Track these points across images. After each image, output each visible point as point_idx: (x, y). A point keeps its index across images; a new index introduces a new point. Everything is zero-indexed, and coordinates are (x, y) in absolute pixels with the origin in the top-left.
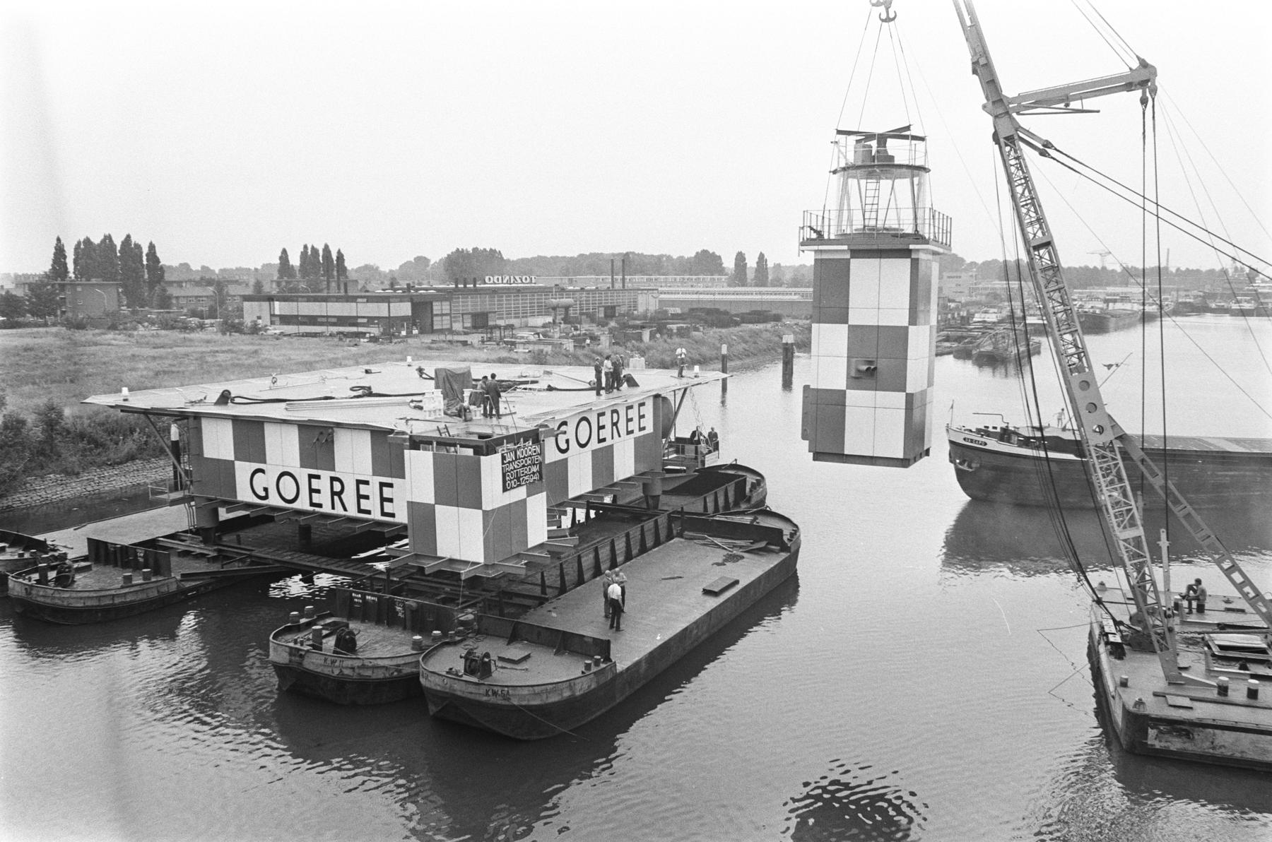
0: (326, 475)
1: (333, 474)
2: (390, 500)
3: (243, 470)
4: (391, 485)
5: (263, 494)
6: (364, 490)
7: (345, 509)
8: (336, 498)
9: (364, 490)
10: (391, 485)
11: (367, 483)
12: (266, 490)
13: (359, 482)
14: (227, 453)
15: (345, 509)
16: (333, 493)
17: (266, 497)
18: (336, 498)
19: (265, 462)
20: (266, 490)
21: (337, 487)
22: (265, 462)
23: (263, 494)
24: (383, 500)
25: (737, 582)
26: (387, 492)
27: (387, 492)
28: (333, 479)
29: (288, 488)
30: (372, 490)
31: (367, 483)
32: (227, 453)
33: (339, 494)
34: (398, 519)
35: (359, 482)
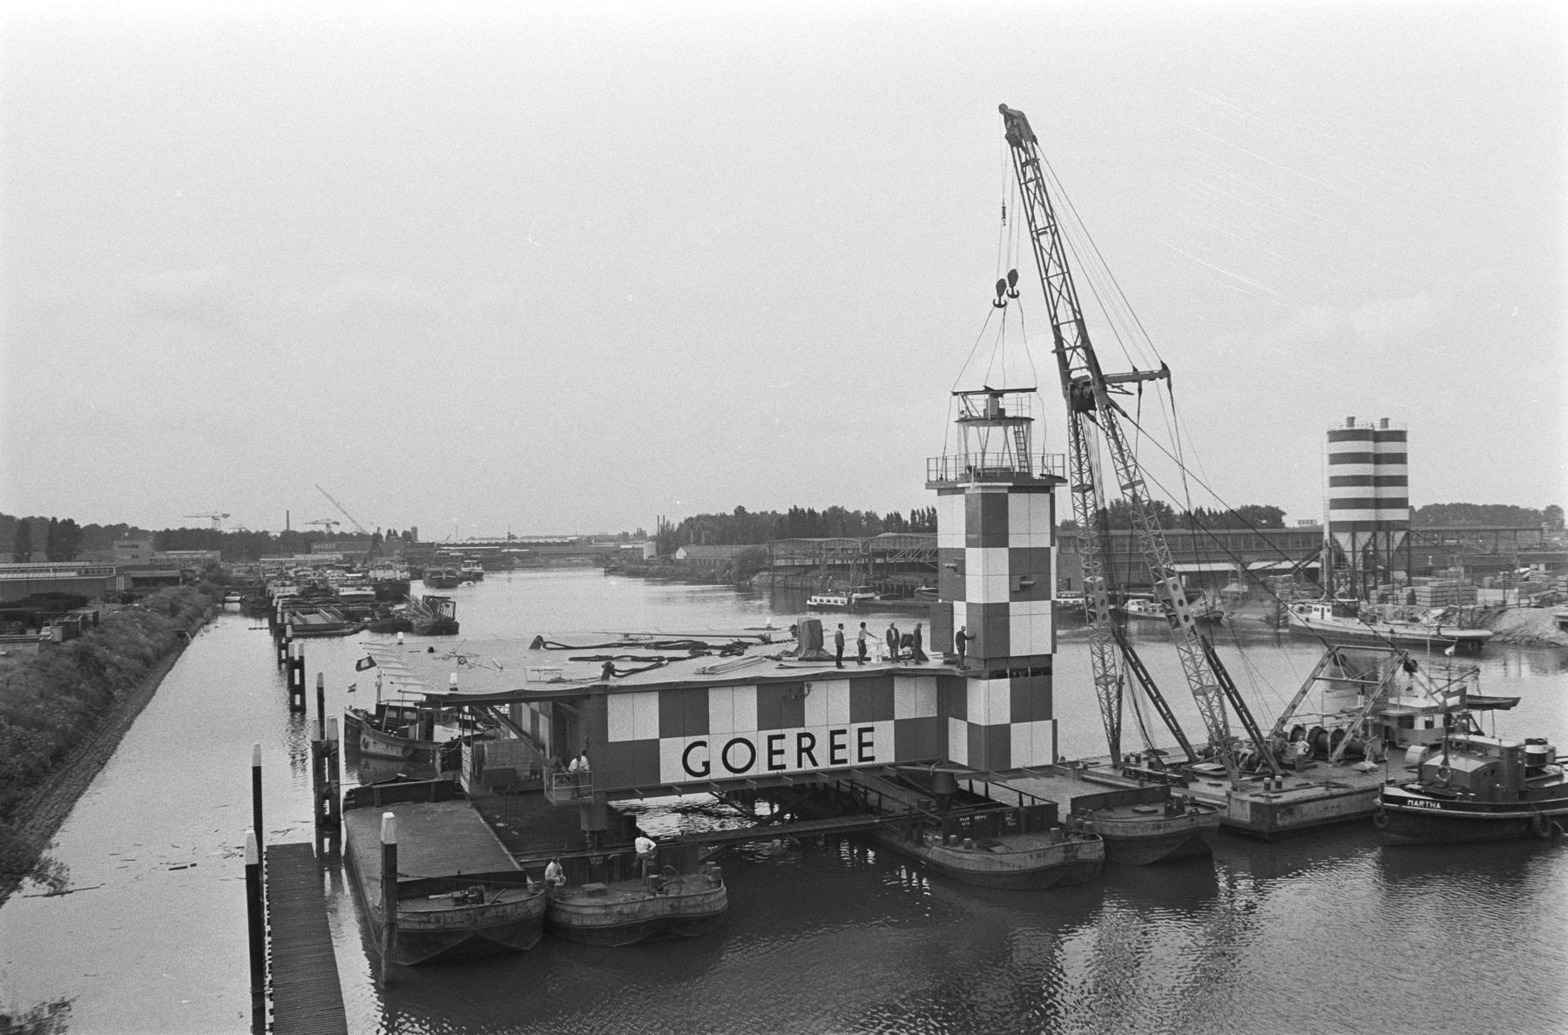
0: (791, 734)
1: (801, 730)
3: (671, 749)
6: (839, 740)
8: (804, 755)
9: (839, 740)
12: (706, 764)
13: (833, 733)
16: (800, 750)
17: (707, 772)
18: (804, 755)
19: (707, 732)
20: (706, 764)
21: (806, 742)
22: (707, 732)
26: (866, 737)
27: (866, 737)
28: (800, 736)
29: (739, 756)
30: (850, 740)
33: (808, 750)
34: (876, 762)
35: (833, 733)
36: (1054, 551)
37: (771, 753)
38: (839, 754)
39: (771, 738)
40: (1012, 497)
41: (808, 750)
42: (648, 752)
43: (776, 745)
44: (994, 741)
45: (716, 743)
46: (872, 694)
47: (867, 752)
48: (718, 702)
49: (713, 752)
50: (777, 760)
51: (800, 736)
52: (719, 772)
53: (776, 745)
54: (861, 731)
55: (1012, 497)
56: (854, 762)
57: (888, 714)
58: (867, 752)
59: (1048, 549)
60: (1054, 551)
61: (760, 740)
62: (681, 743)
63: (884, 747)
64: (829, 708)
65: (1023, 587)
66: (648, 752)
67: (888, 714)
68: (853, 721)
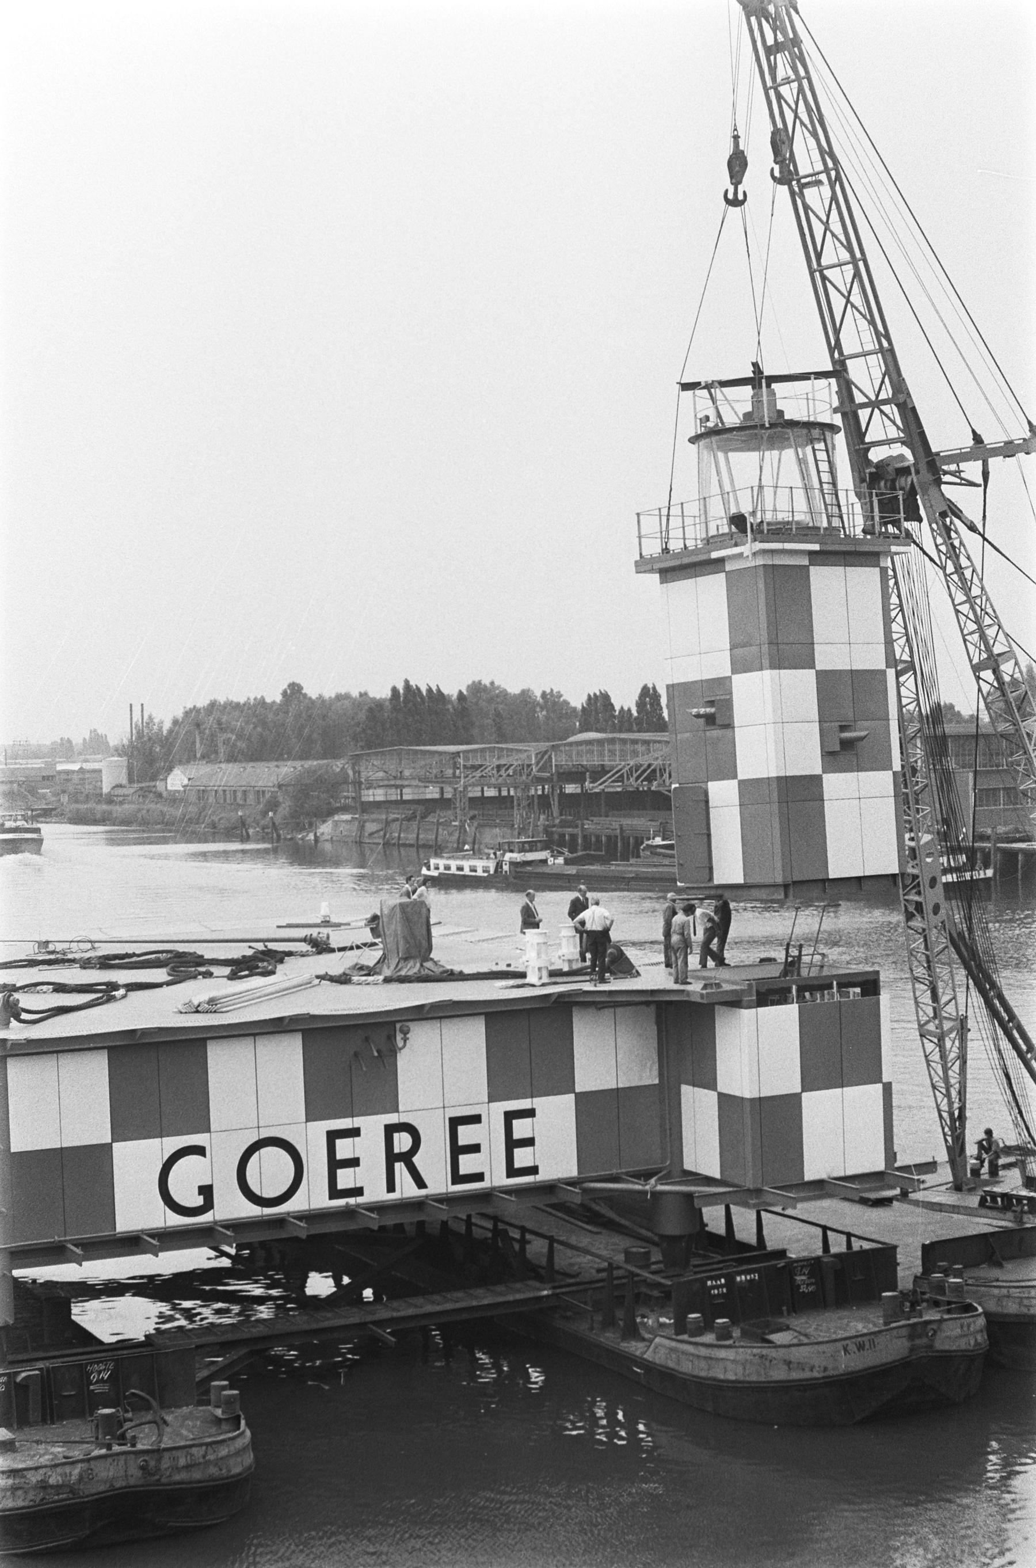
0: (372, 1126)
1: (392, 1118)
2: (529, 1142)
3: (136, 1163)
4: (530, 1113)
5: (199, 1201)
6: (466, 1135)
7: (421, 1183)
8: (399, 1167)
9: (466, 1135)
10: (530, 1113)
11: (476, 1119)
12: (206, 1191)
13: (455, 1123)
15: (421, 1183)
16: (392, 1158)
17: (208, 1205)
18: (399, 1167)
20: (206, 1191)
21: (403, 1142)
22: (208, 1130)
23: (199, 1201)
24: (512, 1144)
26: (521, 1128)
27: (521, 1128)
28: (390, 1130)
29: (271, 1172)
30: (489, 1134)
31: (476, 1119)
33: (407, 1157)
35: (455, 1123)
37: (335, 1164)
38: (468, 1164)
39: (333, 1136)
41: (407, 1157)
42: (90, 1167)
43: (344, 1149)
45: (224, 1145)
47: (523, 1157)
48: (223, 1065)
49: (214, 1167)
50: (346, 1178)
51: (390, 1130)
52: (233, 1206)
53: (344, 1149)
54: (510, 1117)
56: (497, 1178)
57: (563, 1083)
58: (523, 1157)
61: (311, 1142)
63: (554, 1145)
64: (441, 1074)
67: (561, 1081)
68: (492, 1098)
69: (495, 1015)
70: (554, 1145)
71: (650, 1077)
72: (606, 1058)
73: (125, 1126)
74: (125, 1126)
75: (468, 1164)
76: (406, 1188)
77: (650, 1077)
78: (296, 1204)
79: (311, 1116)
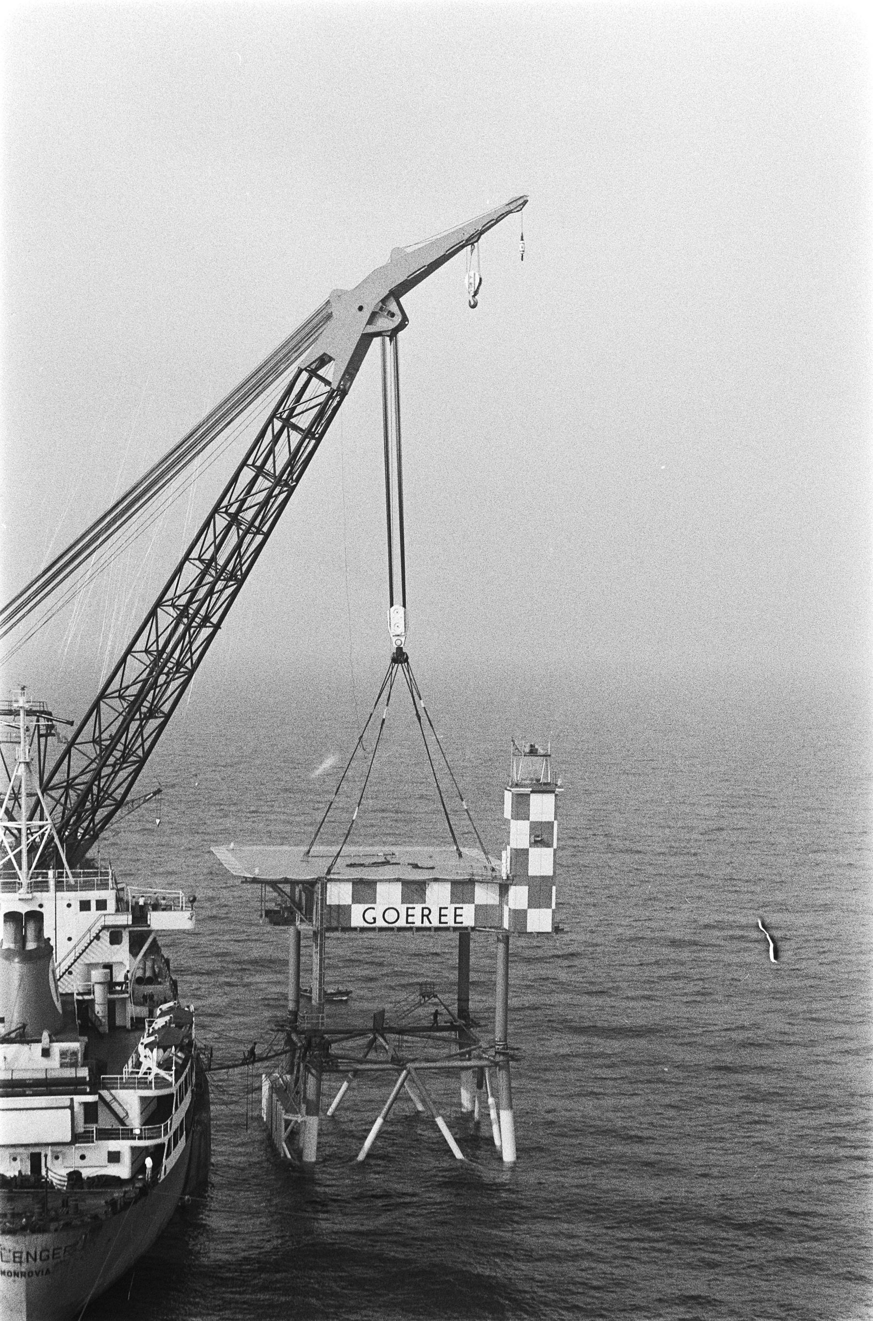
0: (419, 907)
1: (424, 905)
3: (357, 910)
6: (443, 912)
8: (425, 918)
9: (443, 912)
12: (374, 919)
13: (441, 909)
14: (347, 900)
16: (423, 916)
17: (375, 922)
18: (425, 918)
20: (374, 919)
21: (426, 912)
25: (167, 1157)
26: (459, 912)
27: (459, 912)
28: (423, 909)
29: (391, 916)
32: (347, 900)
34: (463, 925)
35: (441, 909)
36: (556, 823)
37: (408, 916)
38: (443, 919)
39: (408, 909)
40: (533, 797)
41: (427, 916)
42: (343, 911)
43: (410, 912)
44: (519, 916)
45: (380, 907)
46: (462, 889)
47: (459, 919)
48: (380, 887)
49: (377, 913)
50: (410, 919)
52: (380, 923)
53: (410, 912)
55: (533, 797)
56: (451, 924)
58: (459, 919)
59: (551, 824)
60: (556, 823)
62: (361, 907)
64: (438, 895)
65: (536, 842)
66: (343, 911)
68: (452, 902)
69: (454, 883)
70: (468, 918)
71: (497, 902)
72: (485, 895)
73: (356, 900)
74: (356, 900)
75: (443, 919)
76: (426, 924)
77: (497, 902)
78: (397, 924)
79: (403, 903)
